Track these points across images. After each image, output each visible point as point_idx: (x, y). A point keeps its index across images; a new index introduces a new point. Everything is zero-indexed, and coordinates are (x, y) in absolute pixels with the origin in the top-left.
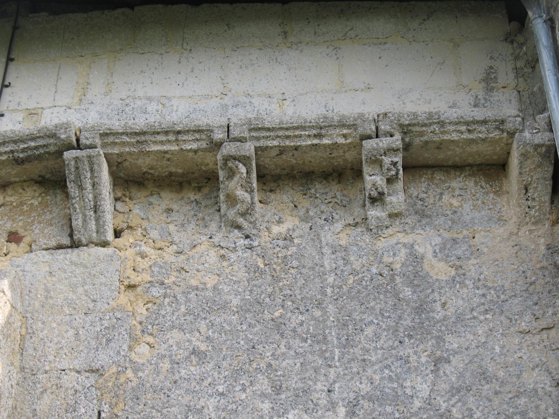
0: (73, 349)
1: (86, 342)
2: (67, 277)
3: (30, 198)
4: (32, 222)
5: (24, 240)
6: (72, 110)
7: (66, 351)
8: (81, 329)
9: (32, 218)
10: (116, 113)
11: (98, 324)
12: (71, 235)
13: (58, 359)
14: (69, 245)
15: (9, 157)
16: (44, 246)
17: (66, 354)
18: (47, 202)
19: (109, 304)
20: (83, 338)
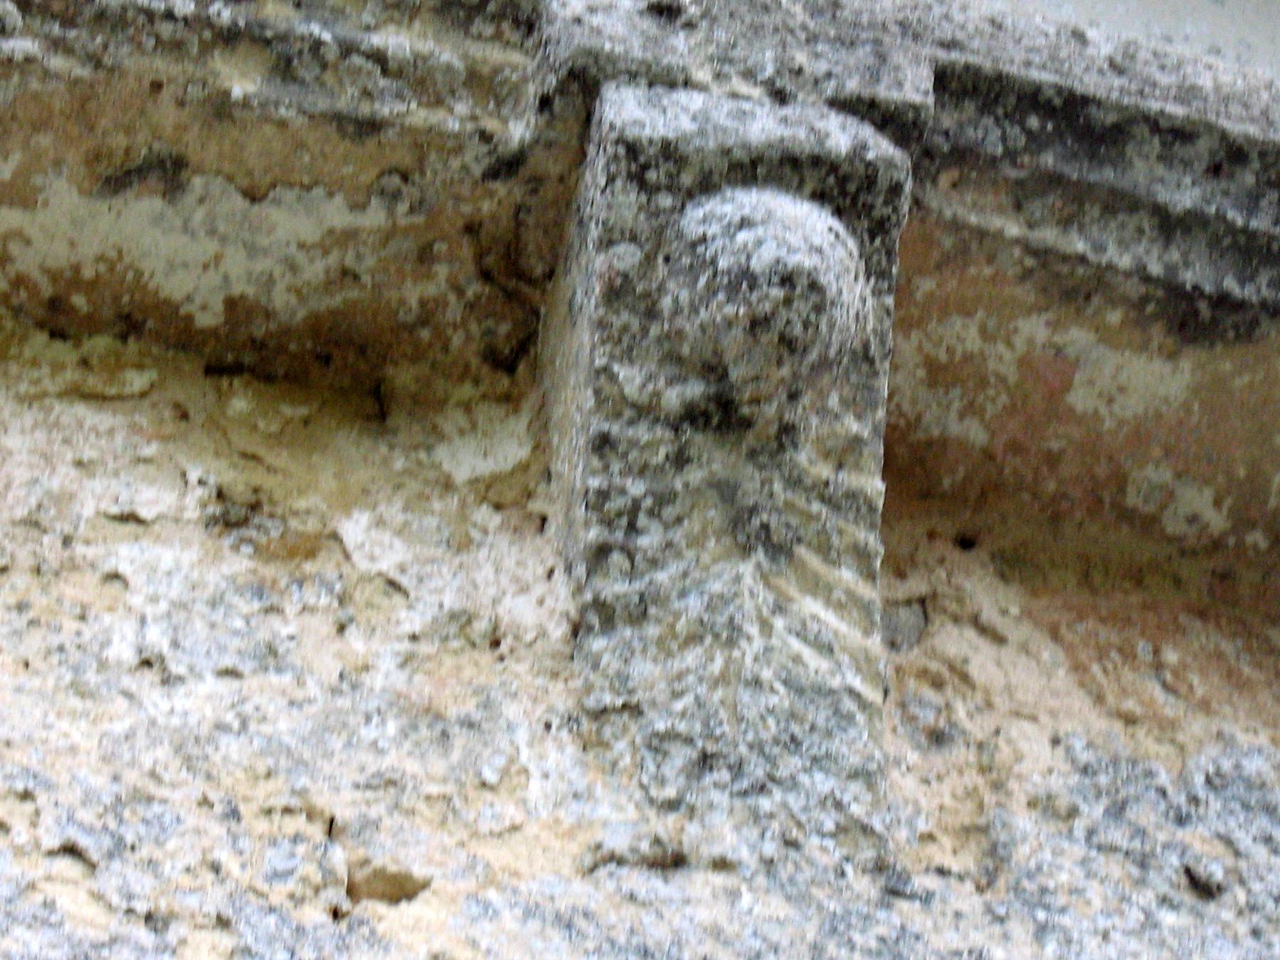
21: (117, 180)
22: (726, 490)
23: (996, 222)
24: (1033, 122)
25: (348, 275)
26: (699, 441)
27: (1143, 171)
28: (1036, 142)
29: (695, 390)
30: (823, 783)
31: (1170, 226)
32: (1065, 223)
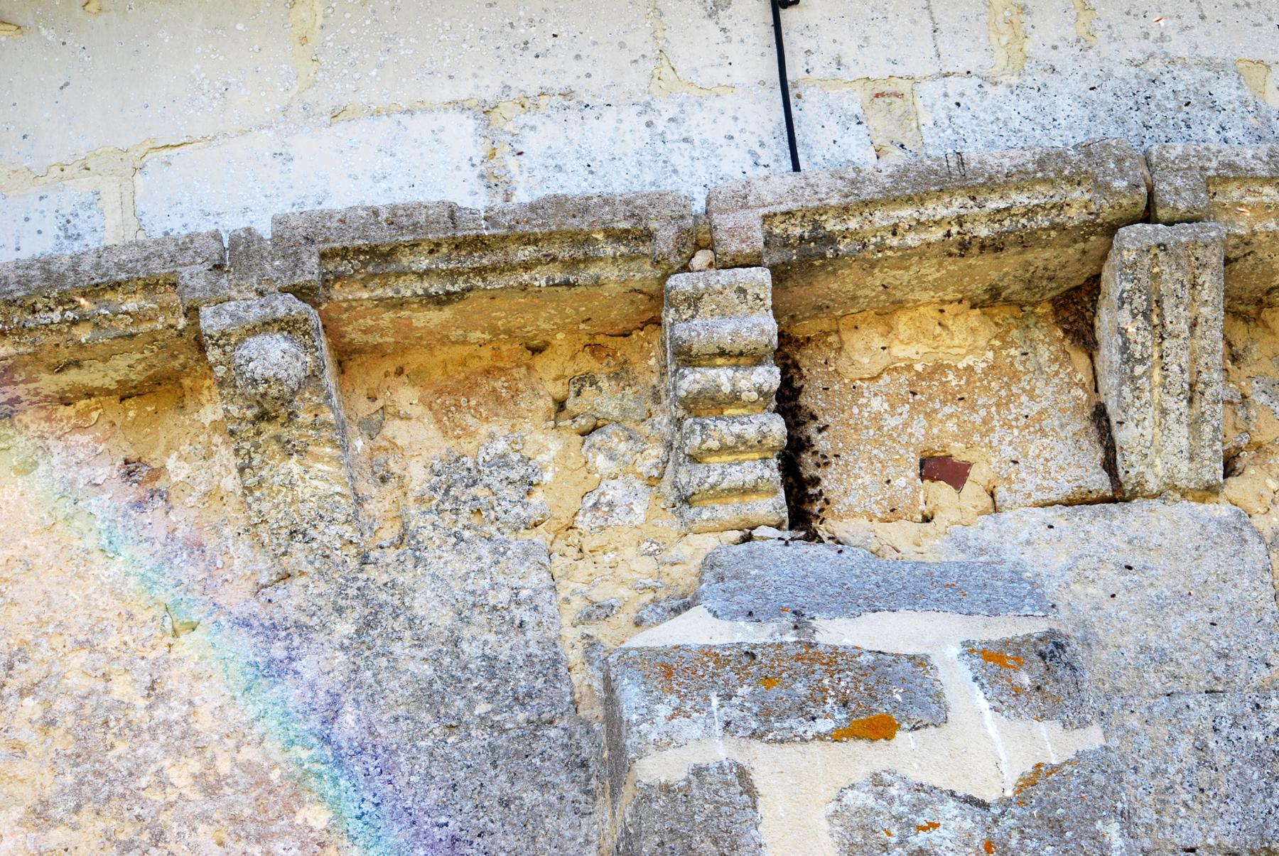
0: (1202, 790)
1: (1235, 772)
2: (1131, 585)
3: (963, 351)
4: (984, 422)
5: (973, 472)
6: (1001, 90)
7: (1187, 797)
8: (1210, 735)
9: (983, 412)
10: (1131, 104)
11: (1255, 722)
12: (1110, 465)
13: (1167, 820)
14: (1110, 494)
15: (949, 234)
16: (1039, 496)
17: (1186, 805)
18: (1012, 364)
19: (1268, 665)
20: (1222, 760)
21: (61, 369)
22: (278, 439)
23: (359, 295)
24: (362, 258)
25: (152, 366)
26: (263, 425)
27: (405, 260)
28: (365, 264)
29: (256, 410)
30: (334, 529)
31: (421, 275)
32: (384, 286)
